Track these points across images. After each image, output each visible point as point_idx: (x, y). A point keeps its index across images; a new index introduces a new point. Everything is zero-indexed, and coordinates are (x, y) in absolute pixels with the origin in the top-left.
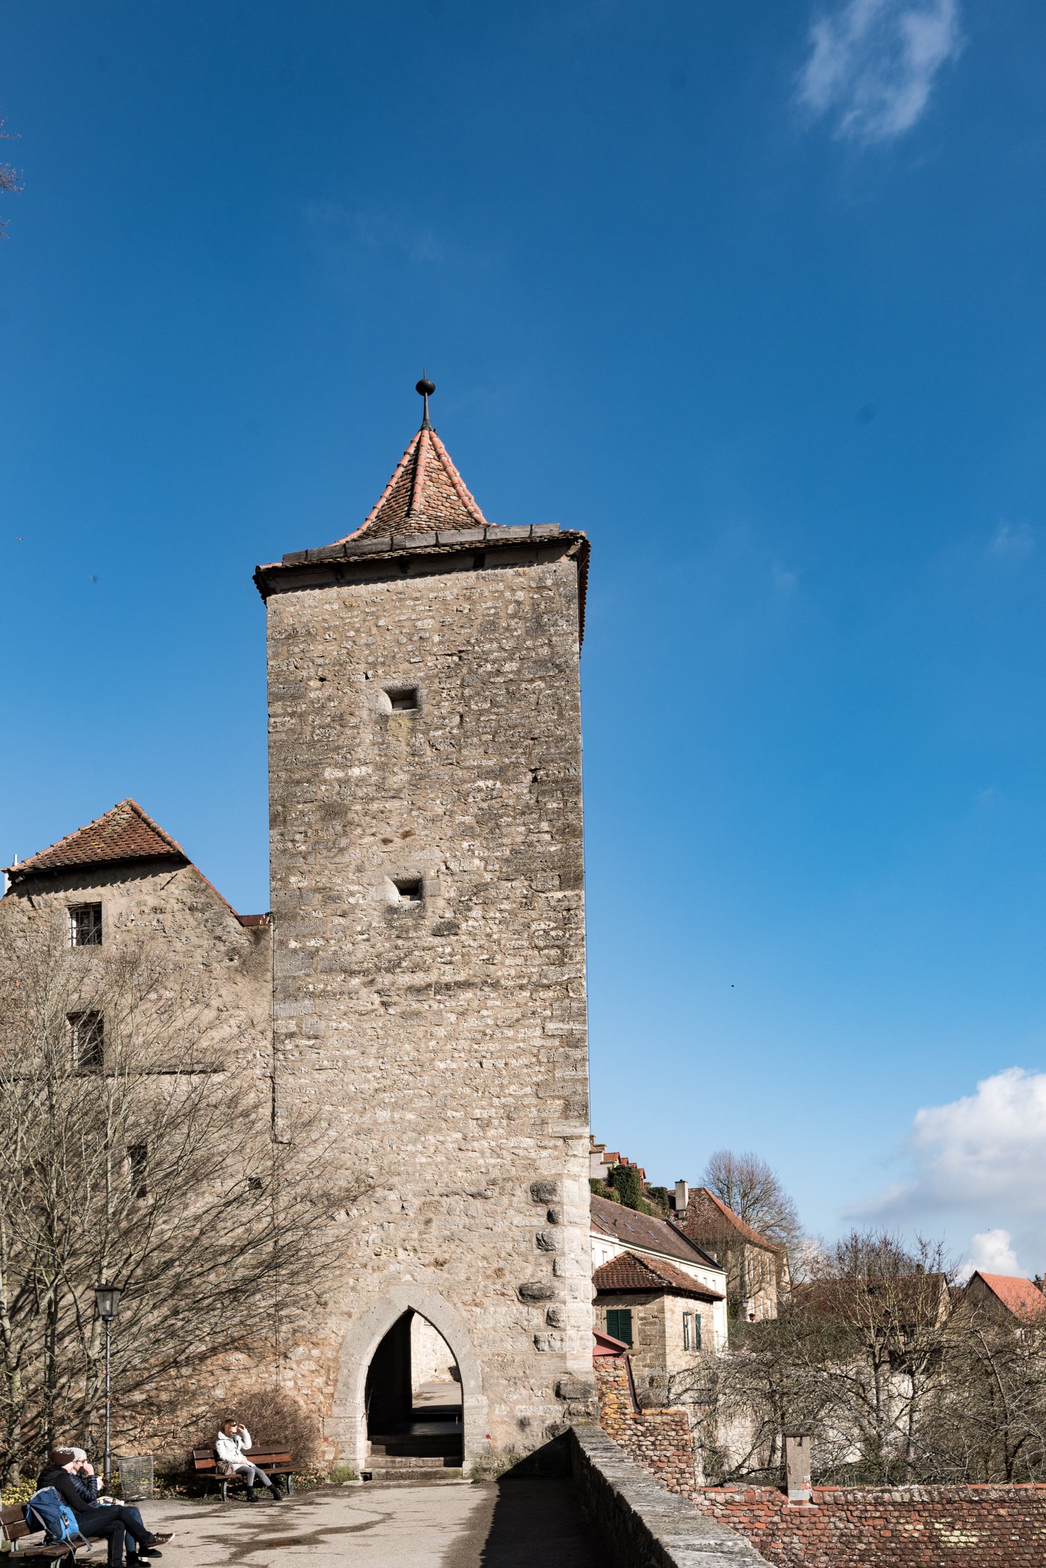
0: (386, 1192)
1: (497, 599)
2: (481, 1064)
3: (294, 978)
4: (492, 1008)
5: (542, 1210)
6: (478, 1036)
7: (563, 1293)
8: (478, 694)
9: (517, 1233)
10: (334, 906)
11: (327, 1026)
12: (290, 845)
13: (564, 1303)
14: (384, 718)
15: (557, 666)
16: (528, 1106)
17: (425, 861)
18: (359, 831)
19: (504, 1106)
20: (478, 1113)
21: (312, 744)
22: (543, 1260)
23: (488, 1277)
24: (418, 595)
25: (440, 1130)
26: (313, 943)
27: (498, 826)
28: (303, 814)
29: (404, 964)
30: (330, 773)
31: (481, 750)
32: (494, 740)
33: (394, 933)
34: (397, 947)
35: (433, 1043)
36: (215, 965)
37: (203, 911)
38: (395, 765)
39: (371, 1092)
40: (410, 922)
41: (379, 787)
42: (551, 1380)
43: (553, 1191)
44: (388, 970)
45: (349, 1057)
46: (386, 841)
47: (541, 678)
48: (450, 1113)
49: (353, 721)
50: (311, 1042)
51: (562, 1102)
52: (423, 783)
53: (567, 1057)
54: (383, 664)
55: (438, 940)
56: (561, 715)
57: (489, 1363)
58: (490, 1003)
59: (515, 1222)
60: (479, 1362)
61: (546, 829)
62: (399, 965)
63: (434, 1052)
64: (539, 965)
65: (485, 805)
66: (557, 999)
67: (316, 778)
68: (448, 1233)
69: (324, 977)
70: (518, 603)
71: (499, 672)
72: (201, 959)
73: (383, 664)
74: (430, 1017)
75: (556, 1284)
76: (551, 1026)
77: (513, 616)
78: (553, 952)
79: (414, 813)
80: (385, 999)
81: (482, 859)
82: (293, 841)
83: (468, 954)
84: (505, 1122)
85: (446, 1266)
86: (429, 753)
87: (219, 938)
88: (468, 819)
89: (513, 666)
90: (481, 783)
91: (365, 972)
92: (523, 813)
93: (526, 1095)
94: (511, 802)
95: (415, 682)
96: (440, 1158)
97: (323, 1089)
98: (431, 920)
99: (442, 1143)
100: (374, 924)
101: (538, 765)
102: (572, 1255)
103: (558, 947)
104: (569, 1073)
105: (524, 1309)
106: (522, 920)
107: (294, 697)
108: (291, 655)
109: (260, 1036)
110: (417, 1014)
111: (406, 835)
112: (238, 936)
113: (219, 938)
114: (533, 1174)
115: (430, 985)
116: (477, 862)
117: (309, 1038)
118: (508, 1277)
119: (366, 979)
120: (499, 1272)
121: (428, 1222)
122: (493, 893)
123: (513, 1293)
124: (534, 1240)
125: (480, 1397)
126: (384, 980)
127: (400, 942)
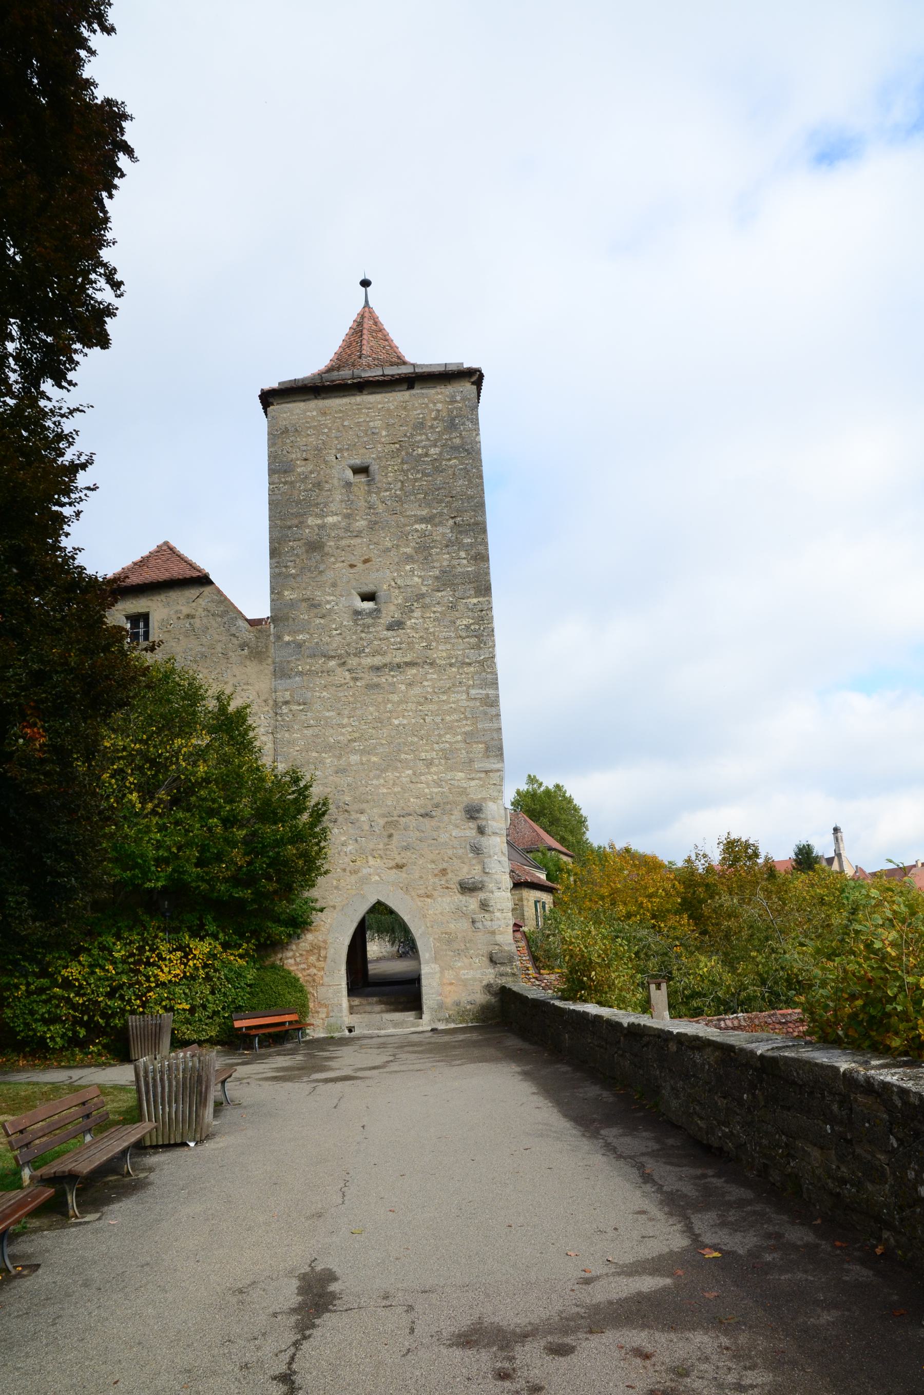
0: (358, 815)
1: (424, 408)
2: (424, 720)
3: (288, 662)
4: (431, 680)
5: (472, 825)
6: (422, 700)
7: (491, 886)
8: (413, 468)
10: (316, 611)
11: (313, 696)
12: (284, 570)
13: (492, 892)
14: (348, 484)
15: (466, 450)
16: (460, 750)
17: (380, 578)
18: (333, 559)
19: (442, 750)
20: (423, 756)
21: (298, 502)
22: (474, 862)
23: (436, 875)
24: (370, 406)
25: (397, 768)
26: (301, 636)
27: (430, 555)
28: (293, 548)
29: (367, 650)
30: (311, 521)
31: (417, 504)
32: (424, 498)
34: (361, 639)
35: (389, 706)
36: (231, 654)
37: (221, 617)
38: (357, 515)
39: (346, 742)
40: (369, 621)
41: (347, 530)
42: (484, 950)
43: (479, 810)
44: (355, 655)
45: (329, 718)
46: (352, 566)
47: (455, 458)
48: (403, 756)
49: (327, 486)
50: (301, 707)
51: (483, 745)
52: (377, 526)
53: (486, 714)
54: (347, 449)
55: (390, 633)
56: (469, 481)
57: (439, 940)
58: (429, 676)
59: (454, 834)
60: (431, 939)
61: (464, 556)
62: (363, 651)
63: (390, 712)
64: (463, 650)
66: (477, 673)
67: (301, 525)
68: (405, 844)
69: (309, 660)
70: (438, 411)
71: (427, 455)
72: (220, 650)
73: (347, 449)
74: (387, 688)
75: (485, 879)
76: (473, 692)
77: (435, 419)
78: (473, 640)
79: (371, 547)
80: (354, 675)
81: (420, 577)
83: (412, 643)
84: (443, 761)
85: (404, 868)
86: (380, 507)
87: (234, 635)
88: (408, 550)
89: (437, 450)
90: (417, 526)
91: (340, 657)
92: (447, 546)
93: (457, 742)
97: (310, 741)
98: (385, 620)
99: (398, 778)
100: (345, 623)
101: (456, 514)
102: (496, 857)
103: (476, 636)
104: (487, 725)
105: (463, 898)
106: (449, 619)
107: (285, 472)
108: (284, 444)
109: (263, 704)
110: (377, 686)
111: (366, 561)
112: (247, 634)
113: (234, 635)
114: (465, 799)
115: (385, 665)
116: (416, 579)
117: (300, 704)
118: (450, 875)
119: (340, 662)
120: (444, 872)
121: (390, 836)
123: (455, 887)
124: (468, 846)
125: (433, 966)
126: (352, 662)
127: (363, 635)
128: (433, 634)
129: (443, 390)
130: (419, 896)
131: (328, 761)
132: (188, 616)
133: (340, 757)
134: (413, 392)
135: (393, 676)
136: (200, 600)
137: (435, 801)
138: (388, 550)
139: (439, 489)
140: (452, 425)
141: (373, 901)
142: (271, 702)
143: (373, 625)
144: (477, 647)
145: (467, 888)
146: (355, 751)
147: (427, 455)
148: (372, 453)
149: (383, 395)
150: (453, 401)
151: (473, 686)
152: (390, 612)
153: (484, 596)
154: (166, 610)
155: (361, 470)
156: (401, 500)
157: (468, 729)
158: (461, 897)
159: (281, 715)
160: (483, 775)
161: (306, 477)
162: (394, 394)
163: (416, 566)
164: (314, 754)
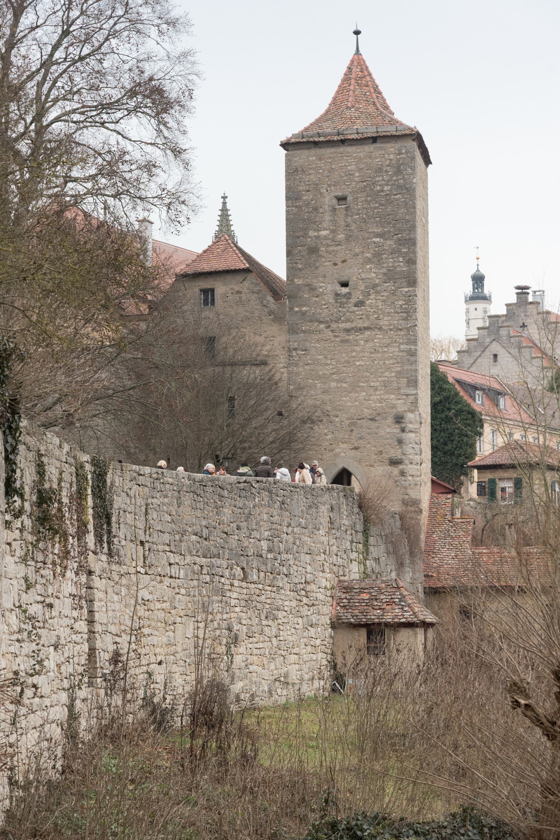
4: (379, 338)
5: (397, 426)
6: (373, 351)
7: (407, 462)
9: (388, 436)
12: (295, 265)
15: (407, 188)
17: (352, 272)
18: (323, 259)
19: (382, 381)
20: (372, 384)
21: (304, 220)
22: (397, 447)
26: (304, 309)
27: (382, 259)
28: (300, 251)
29: (342, 319)
30: (311, 233)
31: (375, 225)
33: (338, 304)
34: (339, 311)
35: (354, 354)
40: (345, 300)
43: (402, 418)
46: (335, 264)
47: (400, 194)
53: (409, 360)
54: (334, 185)
55: (356, 309)
58: (378, 336)
63: (354, 357)
65: (377, 249)
66: (405, 335)
67: (305, 236)
69: (308, 324)
70: (391, 160)
71: (382, 191)
73: (334, 185)
77: (388, 166)
78: (405, 315)
81: (375, 273)
82: (296, 263)
84: (383, 388)
88: (369, 255)
90: (374, 239)
91: (327, 322)
94: (387, 248)
95: (347, 193)
96: (357, 403)
98: (353, 300)
100: (330, 301)
104: (409, 367)
107: (296, 199)
110: (347, 341)
111: (344, 261)
115: (353, 328)
117: (303, 351)
118: (384, 455)
120: (381, 452)
121: (352, 431)
122: (379, 288)
126: (334, 326)
127: (340, 309)
128: (381, 309)
129: (394, 145)
130: (367, 466)
131: (318, 385)
132: (238, 292)
133: (325, 383)
134: (376, 145)
135: (357, 336)
136: (245, 283)
137: (377, 412)
138: (357, 255)
139: (388, 215)
140: (398, 171)
141: (340, 466)
142: (287, 349)
143: (347, 303)
144: (406, 319)
145: (394, 462)
146: (334, 380)
147: (382, 191)
148: (349, 188)
149: (357, 147)
150: (400, 154)
151: (403, 343)
152: (357, 296)
153: (412, 287)
154: (224, 288)
155: (341, 199)
156: (365, 222)
157: (399, 369)
158: (389, 467)
159: (292, 356)
160: (405, 397)
161: (309, 204)
162: (364, 146)
163: (372, 266)
164: (310, 381)
